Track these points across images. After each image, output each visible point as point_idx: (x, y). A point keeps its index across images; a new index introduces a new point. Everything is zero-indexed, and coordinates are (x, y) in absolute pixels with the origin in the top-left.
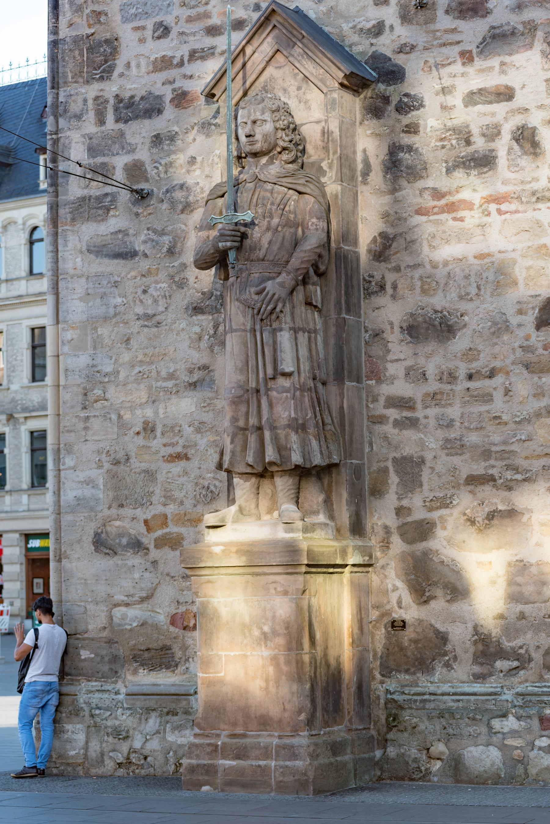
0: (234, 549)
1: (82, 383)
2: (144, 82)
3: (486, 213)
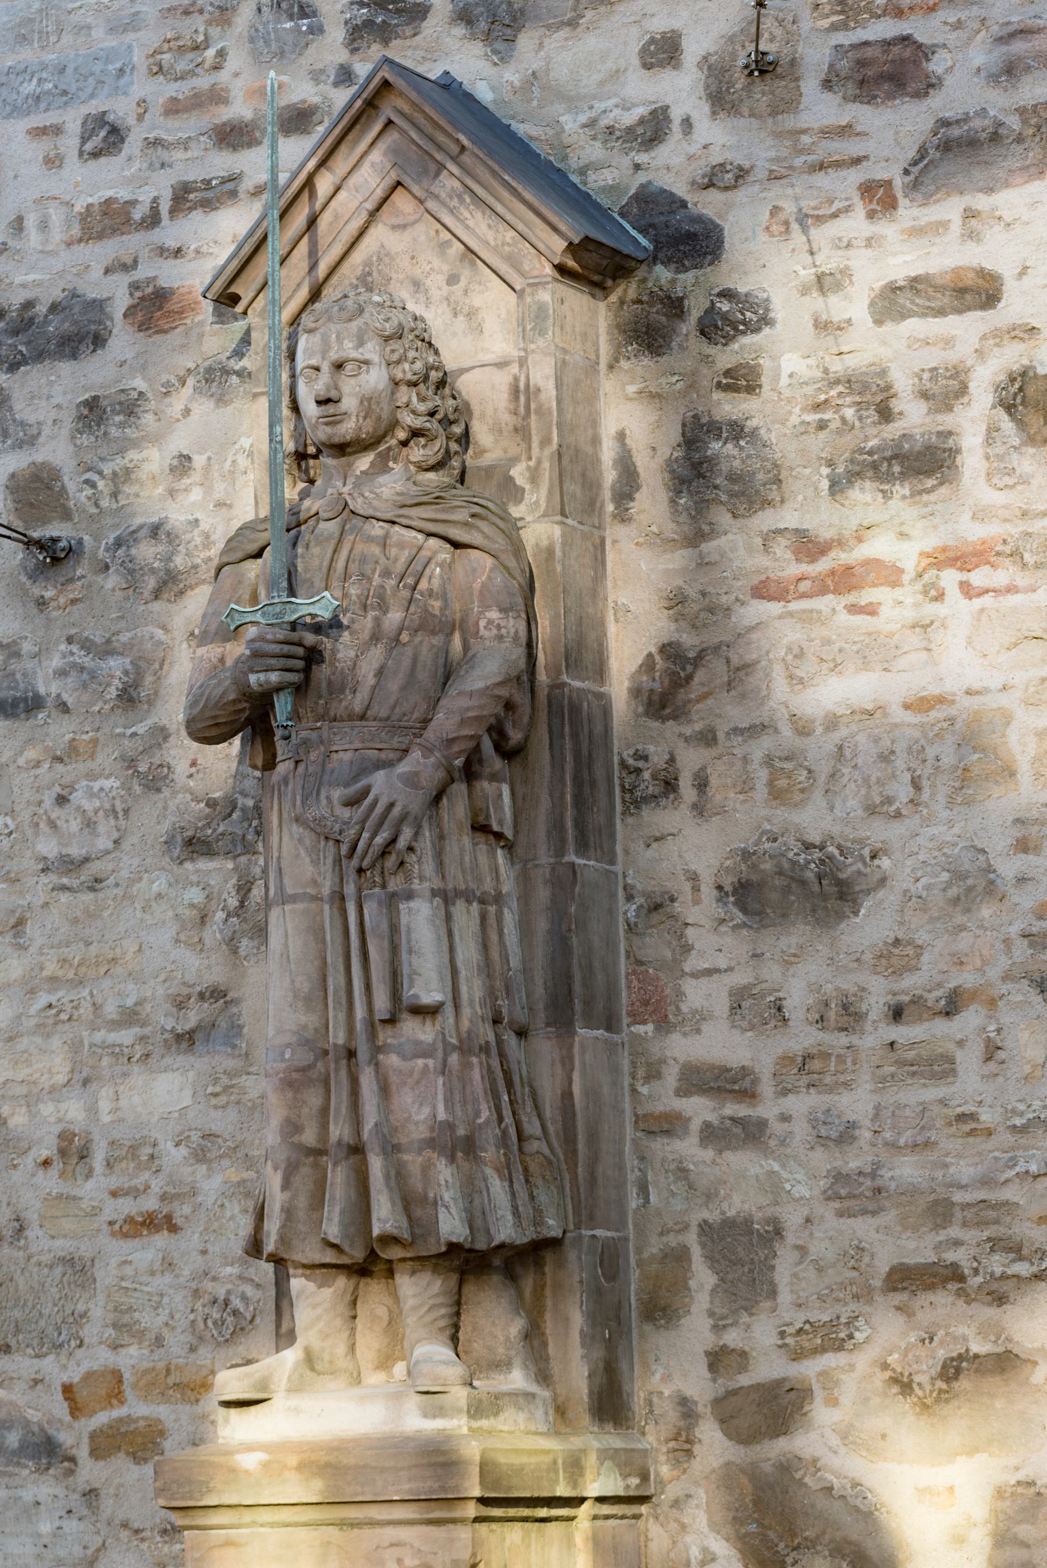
0: (293, 1460)
2: (59, 267)
3: (933, 593)
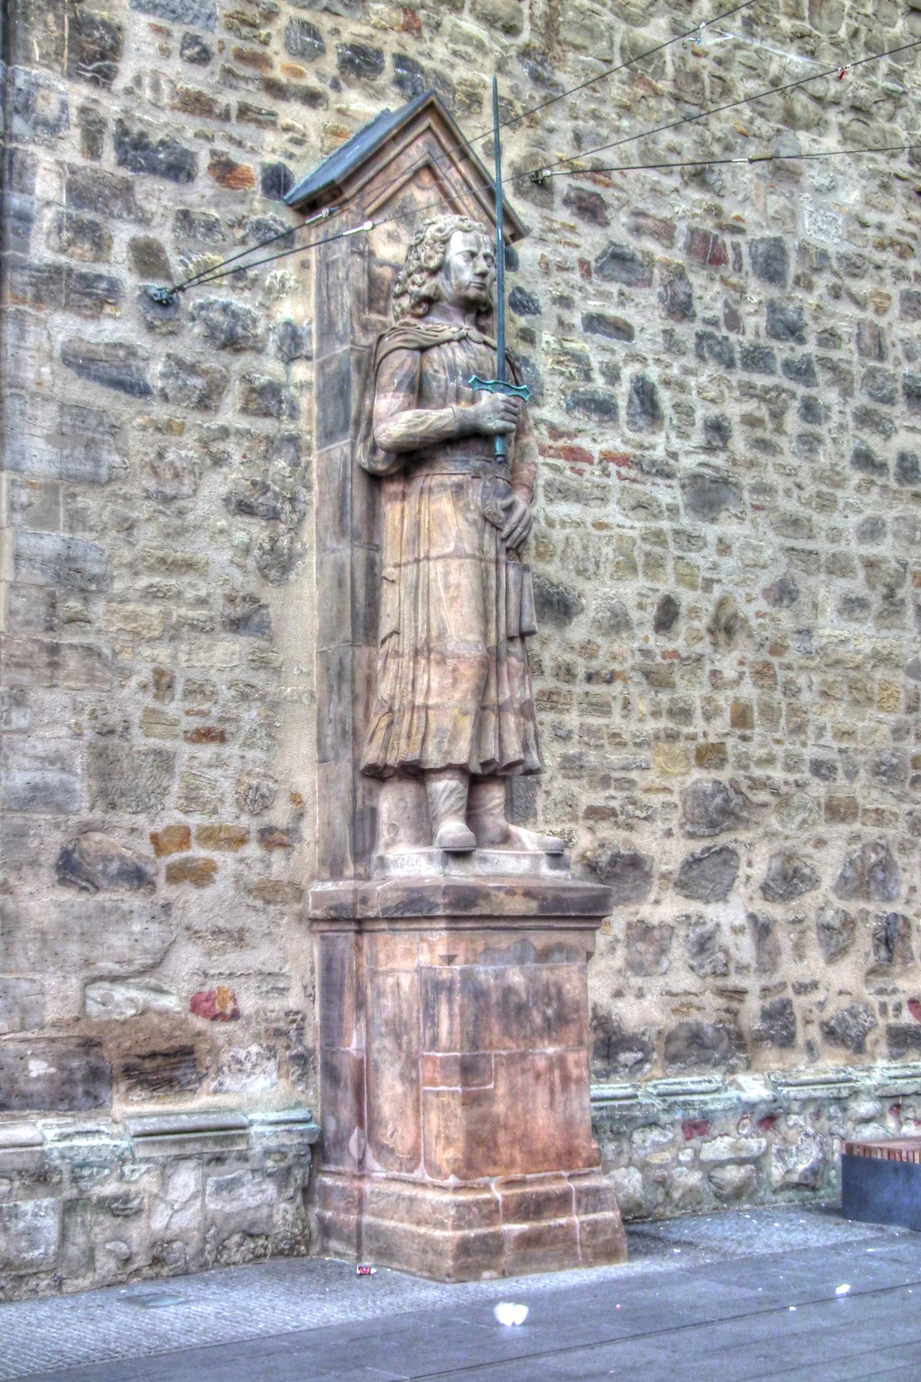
1: (48, 585)
